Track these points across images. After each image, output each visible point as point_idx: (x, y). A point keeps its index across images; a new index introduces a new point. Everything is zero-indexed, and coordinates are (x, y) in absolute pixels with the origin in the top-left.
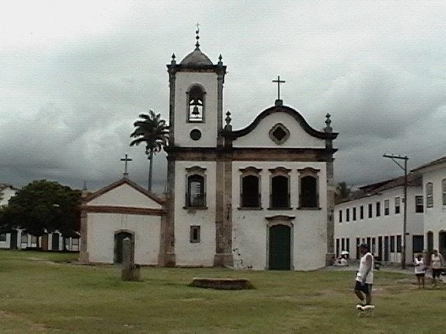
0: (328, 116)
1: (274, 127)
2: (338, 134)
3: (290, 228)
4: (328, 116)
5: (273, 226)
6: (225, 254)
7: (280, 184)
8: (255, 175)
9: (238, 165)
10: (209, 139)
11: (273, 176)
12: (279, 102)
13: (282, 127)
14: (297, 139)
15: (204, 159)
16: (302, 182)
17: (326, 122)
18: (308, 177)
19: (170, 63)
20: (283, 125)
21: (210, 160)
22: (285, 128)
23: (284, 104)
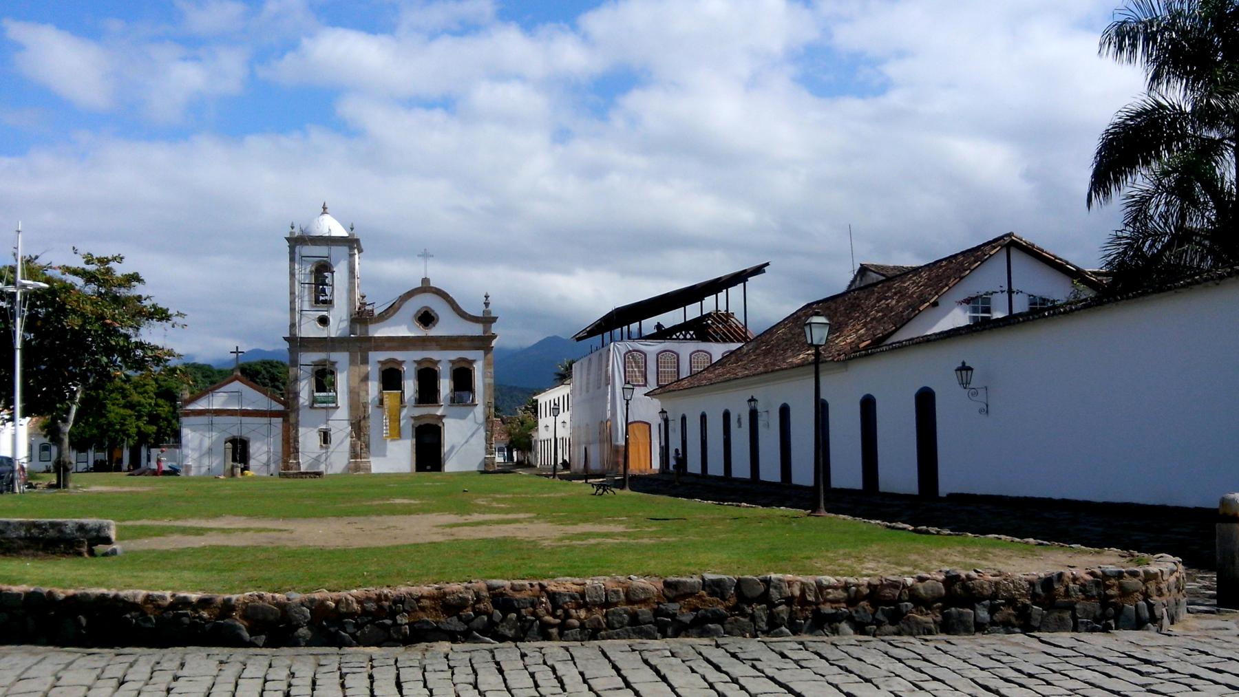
0: (487, 297)
1: (419, 311)
2: (497, 318)
3: (440, 428)
4: (487, 297)
5: (420, 426)
6: (362, 460)
7: (428, 379)
8: (396, 367)
9: (377, 357)
10: (338, 325)
11: (419, 368)
12: (425, 280)
13: (429, 310)
14: (447, 326)
15: (333, 349)
16: (454, 373)
17: (485, 303)
18: (463, 368)
19: (288, 236)
20: (430, 309)
21: (341, 350)
22: (433, 311)
23: (432, 285)
